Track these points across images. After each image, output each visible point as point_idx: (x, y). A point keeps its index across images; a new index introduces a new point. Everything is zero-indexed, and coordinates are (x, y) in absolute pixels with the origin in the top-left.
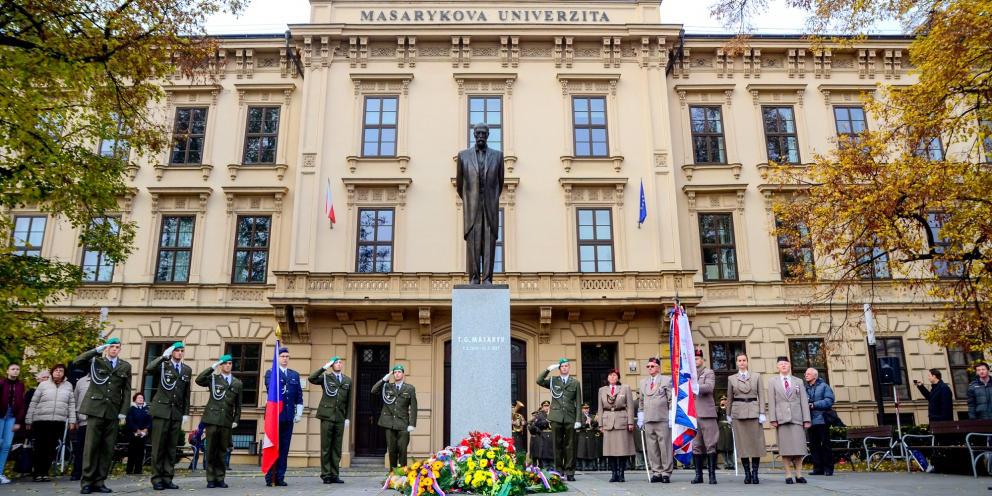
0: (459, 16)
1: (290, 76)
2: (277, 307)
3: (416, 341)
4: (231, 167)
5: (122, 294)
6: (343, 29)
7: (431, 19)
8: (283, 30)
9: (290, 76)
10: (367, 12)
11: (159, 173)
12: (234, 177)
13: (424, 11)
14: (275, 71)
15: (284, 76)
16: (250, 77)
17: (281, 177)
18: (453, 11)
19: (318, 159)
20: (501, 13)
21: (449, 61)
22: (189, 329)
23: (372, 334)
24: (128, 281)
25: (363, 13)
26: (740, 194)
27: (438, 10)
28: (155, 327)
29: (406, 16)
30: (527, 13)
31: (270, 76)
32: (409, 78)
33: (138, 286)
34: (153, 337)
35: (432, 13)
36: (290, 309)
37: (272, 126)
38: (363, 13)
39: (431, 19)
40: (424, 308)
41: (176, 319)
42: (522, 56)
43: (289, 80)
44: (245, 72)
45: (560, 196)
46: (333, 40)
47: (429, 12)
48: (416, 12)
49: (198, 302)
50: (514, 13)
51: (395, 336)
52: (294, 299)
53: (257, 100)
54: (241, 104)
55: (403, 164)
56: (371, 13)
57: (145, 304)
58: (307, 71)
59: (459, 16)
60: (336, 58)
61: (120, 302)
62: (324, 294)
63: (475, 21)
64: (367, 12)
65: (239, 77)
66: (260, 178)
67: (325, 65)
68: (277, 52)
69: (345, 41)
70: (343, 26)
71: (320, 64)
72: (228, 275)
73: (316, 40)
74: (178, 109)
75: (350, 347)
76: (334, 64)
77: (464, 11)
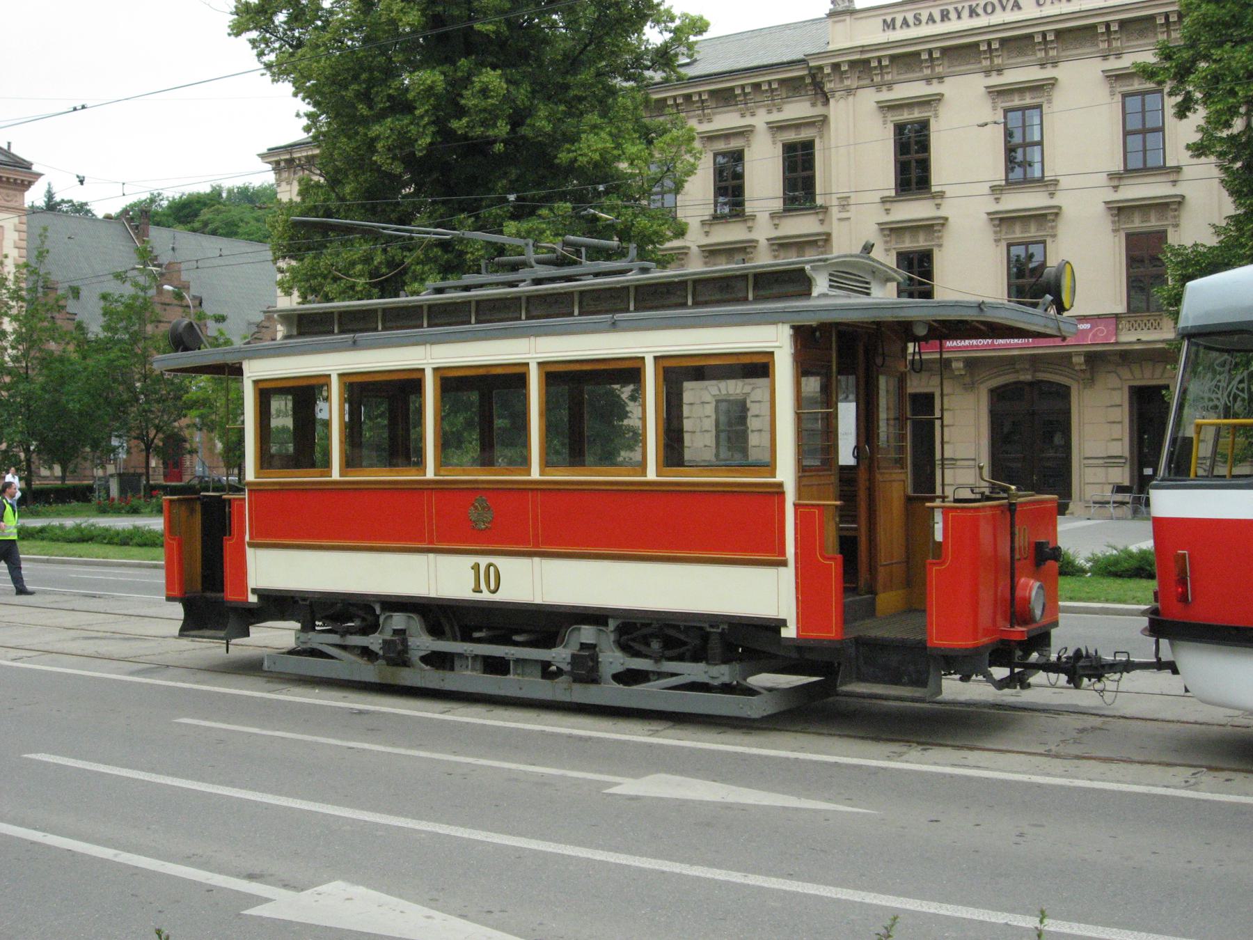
1: (819, 104)
4: (773, 216)
9: (819, 104)
10: (889, 19)
12: (776, 226)
13: (951, 8)
14: (805, 100)
15: (813, 105)
16: (780, 110)
17: (822, 221)
25: (885, 21)
31: (798, 109)
35: (960, 8)
38: (885, 21)
42: (1063, 50)
43: (819, 110)
44: (774, 105)
46: (853, 64)
47: (956, 9)
48: (942, 11)
53: (791, 136)
54: (774, 143)
56: (893, 20)
58: (832, 101)
64: (889, 19)
65: (769, 112)
68: (802, 78)
69: (867, 61)
73: (836, 66)
74: (716, 155)
76: (859, 91)
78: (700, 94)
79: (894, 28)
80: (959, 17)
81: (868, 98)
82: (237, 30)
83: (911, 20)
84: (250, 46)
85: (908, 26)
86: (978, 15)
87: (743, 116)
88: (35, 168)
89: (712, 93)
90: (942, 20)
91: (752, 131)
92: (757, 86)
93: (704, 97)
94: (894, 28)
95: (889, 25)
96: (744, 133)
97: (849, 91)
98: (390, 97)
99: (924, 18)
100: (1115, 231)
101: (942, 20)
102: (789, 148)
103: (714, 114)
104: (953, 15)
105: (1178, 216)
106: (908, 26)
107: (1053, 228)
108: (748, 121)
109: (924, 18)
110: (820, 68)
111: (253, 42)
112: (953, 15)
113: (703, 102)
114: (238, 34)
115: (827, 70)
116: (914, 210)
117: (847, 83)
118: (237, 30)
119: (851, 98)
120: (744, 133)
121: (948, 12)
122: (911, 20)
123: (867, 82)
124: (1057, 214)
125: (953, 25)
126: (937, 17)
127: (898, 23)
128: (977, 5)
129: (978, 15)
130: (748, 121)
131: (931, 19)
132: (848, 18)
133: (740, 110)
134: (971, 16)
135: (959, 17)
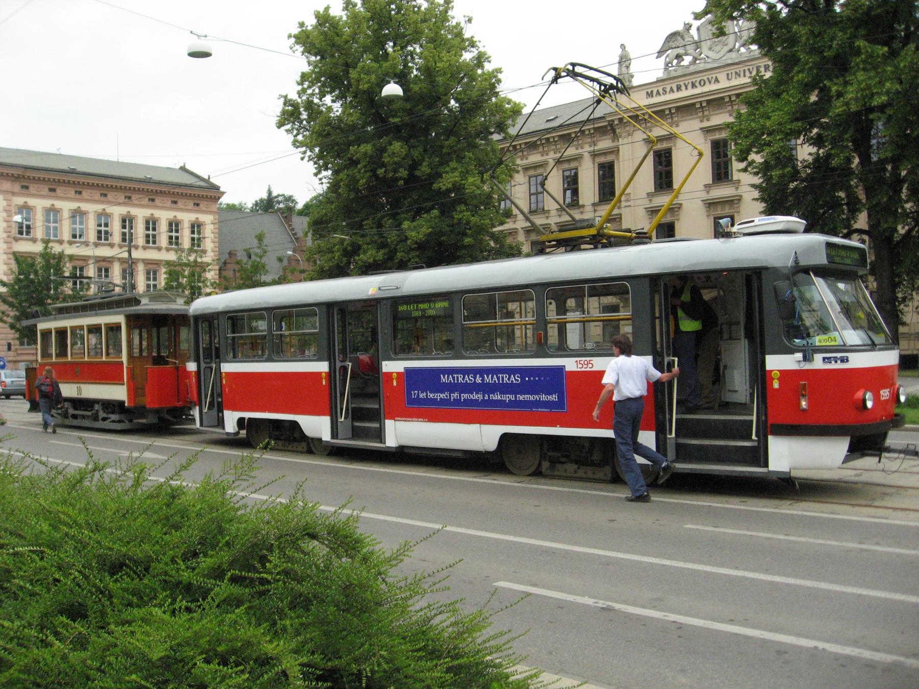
4: (594, 205)
10: (649, 91)
13: (682, 83)
18: (698, 80)
20: (728, 74)
21: (698, 118)
25: (647, 93)
30: (744, 71)
31: (605, 143)
47: (685, 84)
48: (677, 86)
50: (736, 73)
53: (602, 159)
56: (652, 91)
64: (649, 91)
67: (629, 135)
68: (606, 126)
78: (554, 137)
79: (652, 96)
80: (686, 89)
81: (639, 136)
82: (280, 125)
83: (661, 91)
84: (286, 133)
85: (660, 95)
86: (696, 87)
87: (542, 155)
88: (222, 189)
89: (561, 137)
90: (678, 91)
91: (581, 157)
93: (556, 139)
94: (652, 96)
95: (650, 95)
96: (578, 158)
98: (350, 159)
99: (668, 90)
100: (708, 216)
101: (678, 91)
102: (602, 166)
103: (529, 155)
104: (683, 88)
105: (739, 207)
106: (660, 95)
107: (677, 215)
109: (668, 90)
110: (613, 121)
111: (287, 131)
112: (683, 88)
113: (556, 141)
114: (279, 127)
115: (616, 122)
116: (663, 200)
118: (280, 125)
120: (578, 158)
122: (661, 91)
124: (739, 200)
125: (684, 93)
126: (675, 89)
127: (654, 94)
129: (696, 87)
130: (580, 151)
131: (672, 90)
133: (540, 152)
134: (693, 87)
135: (686, 89)
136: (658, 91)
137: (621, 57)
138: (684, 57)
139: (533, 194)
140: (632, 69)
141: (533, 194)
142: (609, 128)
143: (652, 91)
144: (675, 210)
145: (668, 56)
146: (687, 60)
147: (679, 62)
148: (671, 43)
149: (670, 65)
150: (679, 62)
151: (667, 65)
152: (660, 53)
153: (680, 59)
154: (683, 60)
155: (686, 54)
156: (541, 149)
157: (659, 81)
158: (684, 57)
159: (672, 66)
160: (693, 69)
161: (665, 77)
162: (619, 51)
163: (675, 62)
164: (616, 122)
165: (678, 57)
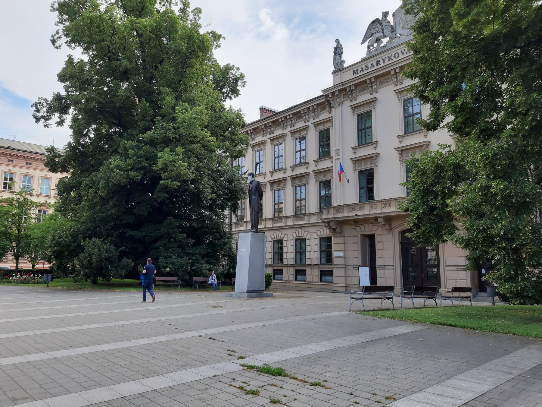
0: (397, 55)
2: (325, 222)
3: (385, 232)
5: (286, 221)
6: (343, 85)
7: (384, 62)
8: (322, 94)
10: (355, 70)
11: (400, 140)
13: (380, 59)
18: (394, 53)
19: (341, 151)
22: (307, 232)
23: (368, 230)
24: (288, 215)
25: (354, 71)
26: (331, 171)
27: (387, 56)
28: (322, 230)
29: (372, 65)
31: (324, 116)
32: (375, 99)
33: (290, 217)
34: (297, 237)
36: (328, 222)
37: (328, 139)
38: (354, 71)
39: (384, 62)
40: (380, 217)
41: (303, 229)
45: (396, 154)
46: (340, 91)
48: (377, 61)
49: (309, 221)
51: (376, 231)
52: (329, 218)
53: (321, 128)
54: (316, 131)
55: (375, 146)
56: (357, 70)
57: (293, 224)
59: (397, 55)
60: (345, 99)
61: (286, 224)
62: (346, 214)
63: (405, 56)
66: (325, 164)
67: (340, 105)
69: (345, 89)
70: (342, 84)
71: (338, 105)
72: (318, 208)
73: (333, 93)
75: (359, 237)
76: (344, 103)
77: (399, 52)
81: (347, 104)
92: (308, 109)
96: (306, 128)
97: (340, 104)
108: (307, 124)
117: (339, 100)
119: (340, 107)
121: (379, 61)
122: (364, 68)
123: (347, 98)
128: (391, 55)
132: (339, 73)
136: (362, 68)
137: (336, 49)
138: (382, 40)
139: (277, 157)
140: (344, 57)
141: (277, 157)
142: (327, 103)
143: (357, 70)
144: (374, 158)
145: (370, 42)
146: (385, 41)
147: (379, 45)
148: (372, 30)
149: (371, 48)
150: (379, 45)
151: (369, 47)
152: (363, 42)
153: (380, 42)
154: (382, 42)
155: (385, 37)
156: (282, 125)
157: (363, 60)
158: (382, 40)
159: (374, 48)
160: (390, 46)
161: (368, 57)
162: (335, 45)
163: (375, 45)
164: (330, 96)
165: (378, 40)
